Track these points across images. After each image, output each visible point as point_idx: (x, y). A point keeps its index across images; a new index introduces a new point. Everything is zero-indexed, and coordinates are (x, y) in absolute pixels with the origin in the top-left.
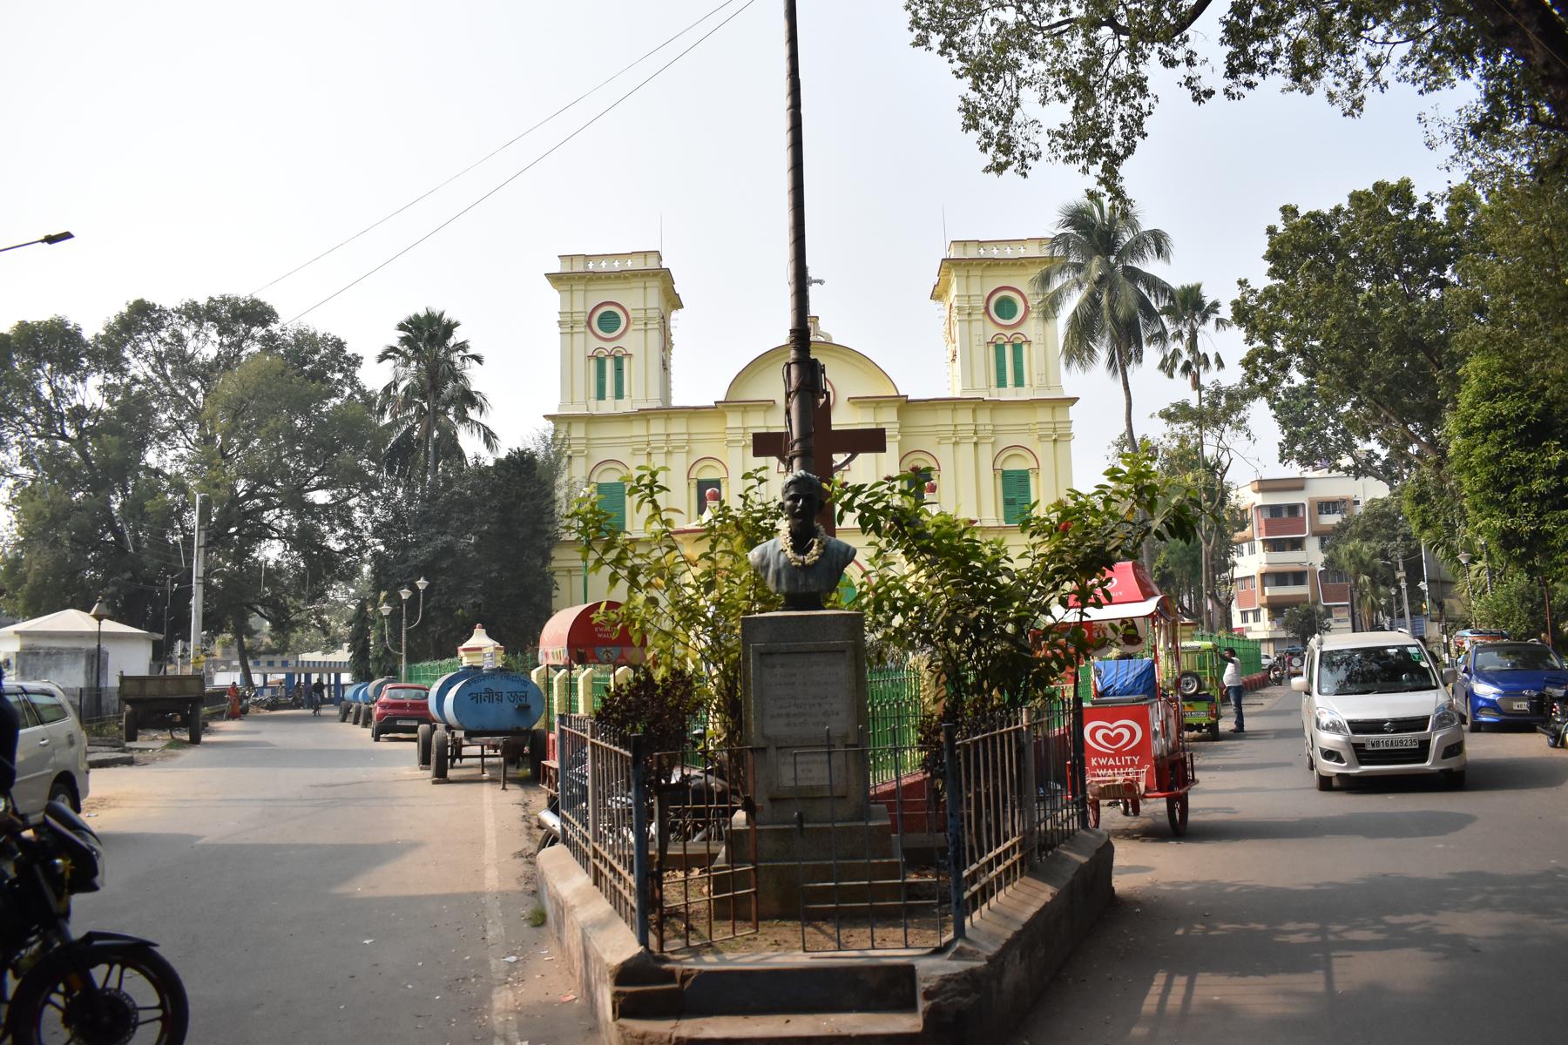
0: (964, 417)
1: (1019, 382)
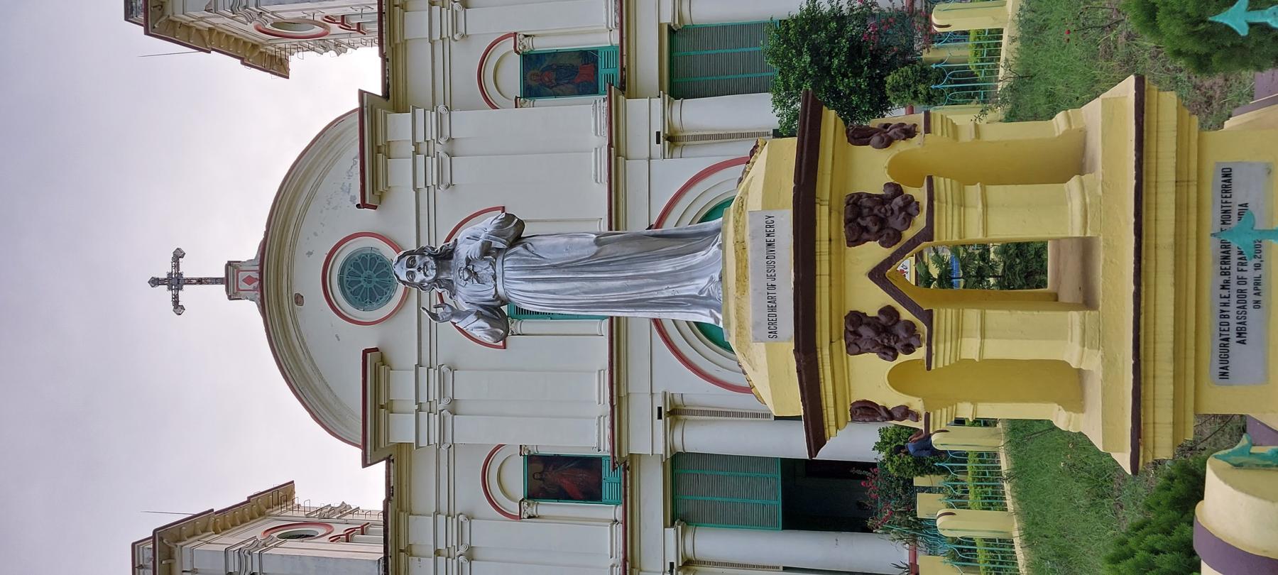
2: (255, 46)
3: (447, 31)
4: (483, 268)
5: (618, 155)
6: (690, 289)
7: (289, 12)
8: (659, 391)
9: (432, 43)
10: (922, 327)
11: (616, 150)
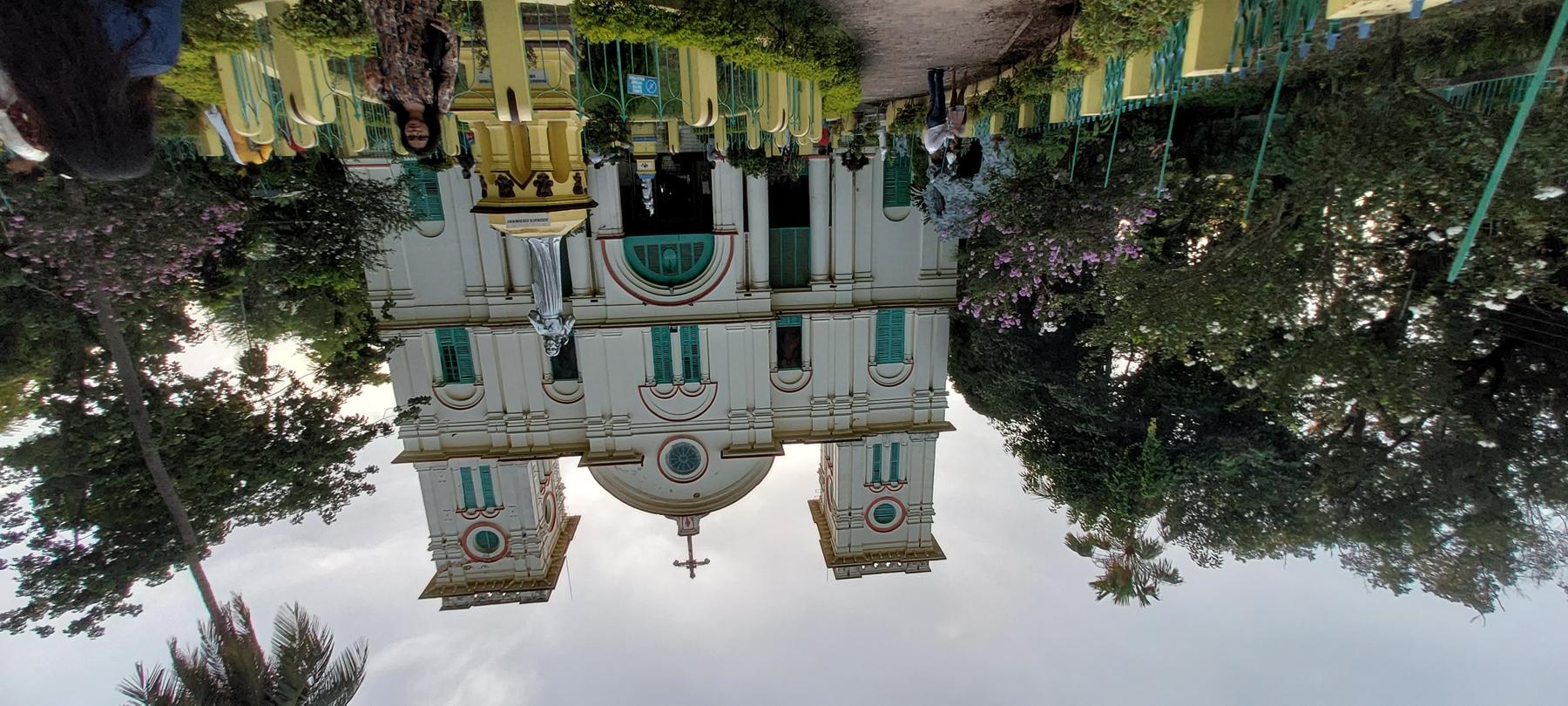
0: (519, 440)
1: (466, 472)
2: (562, 534)
3: (543, 421)
4: (548, 323)
5: (605, 323)
6: (547, 250)
7: (539, 513)
8: (735, 296)
9: (550, 430)
10: (538, 173)
11: (603, 324)
